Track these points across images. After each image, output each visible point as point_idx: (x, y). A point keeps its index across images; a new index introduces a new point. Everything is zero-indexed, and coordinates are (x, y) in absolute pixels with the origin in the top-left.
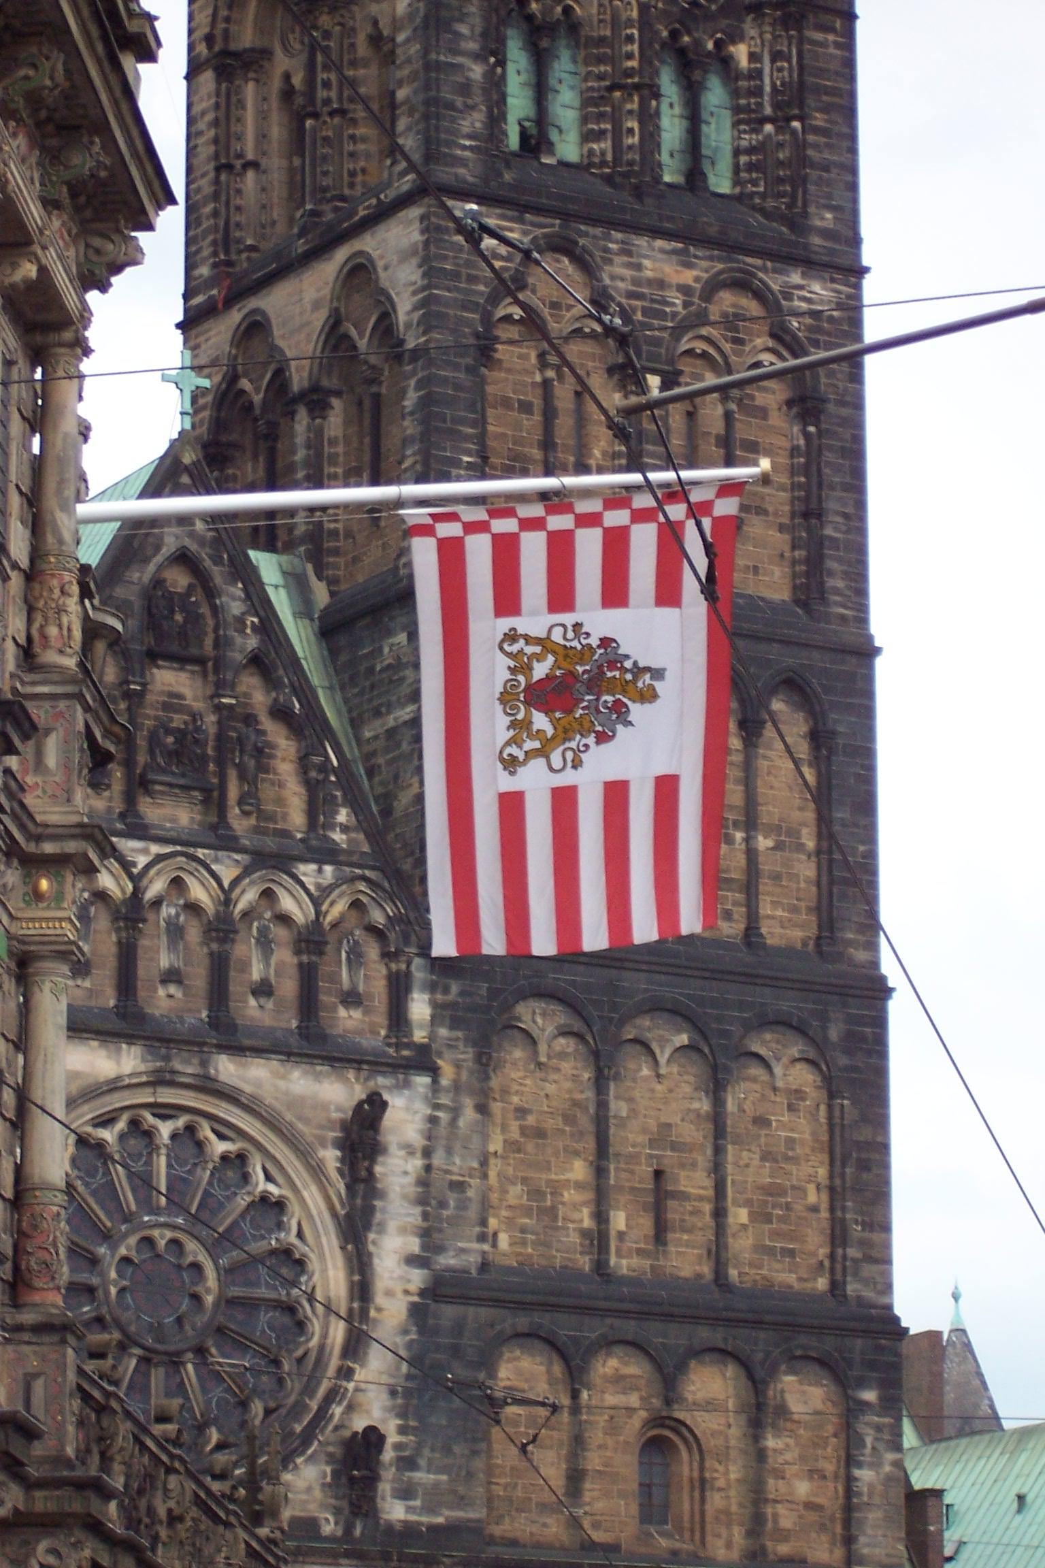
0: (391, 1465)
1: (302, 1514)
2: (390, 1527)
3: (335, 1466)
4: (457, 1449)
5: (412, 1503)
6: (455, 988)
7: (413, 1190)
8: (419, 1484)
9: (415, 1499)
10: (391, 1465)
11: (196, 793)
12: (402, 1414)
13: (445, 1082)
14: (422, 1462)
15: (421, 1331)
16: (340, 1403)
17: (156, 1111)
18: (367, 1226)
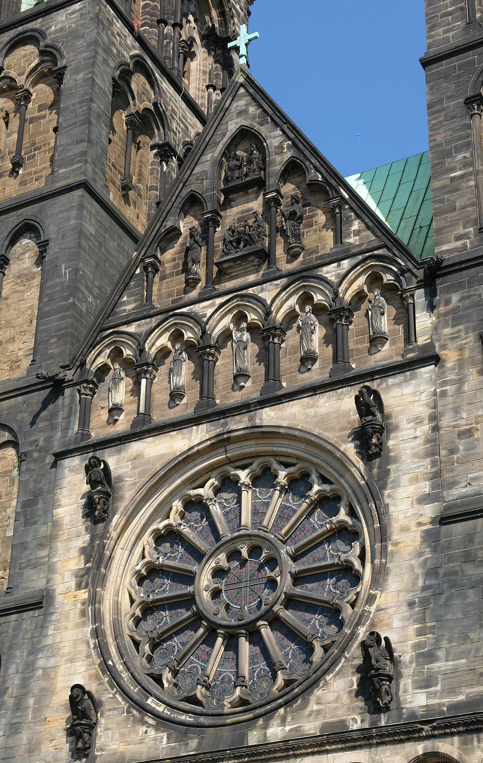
0: (411, 662)
1: (333, 720)
2: (413, 714)
3: (359, 675)
4: (472, 635)
5: (433, 689)
6: (455, 298)
7: (422, 449)
8: (438, 672)
9: (436, 685)
10: (411, 662)
11: (252, 258)
12: (423, 620)
13: (449, 365)
14: (441, 654)
15: (434, 550)
16: (364, 625)
17: (237, 464)
18: (383, 487)
